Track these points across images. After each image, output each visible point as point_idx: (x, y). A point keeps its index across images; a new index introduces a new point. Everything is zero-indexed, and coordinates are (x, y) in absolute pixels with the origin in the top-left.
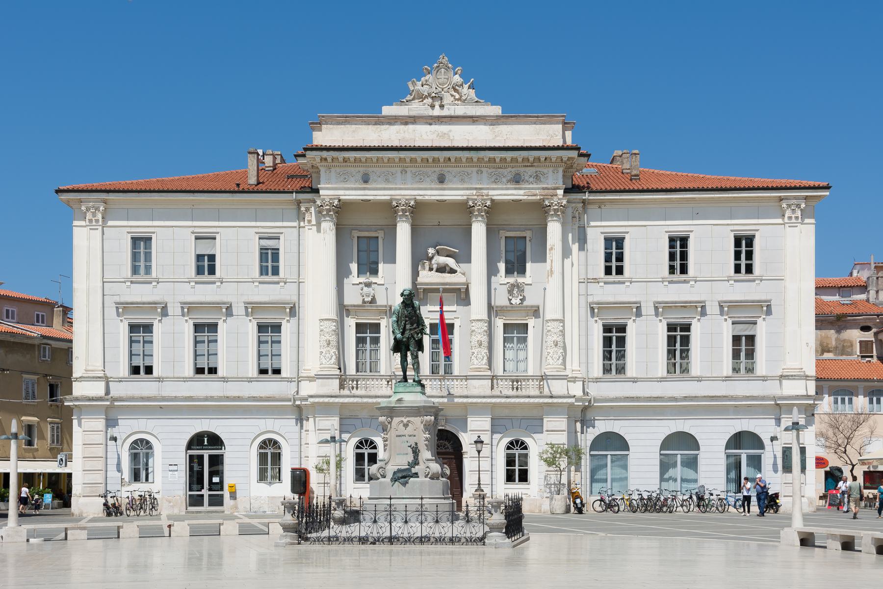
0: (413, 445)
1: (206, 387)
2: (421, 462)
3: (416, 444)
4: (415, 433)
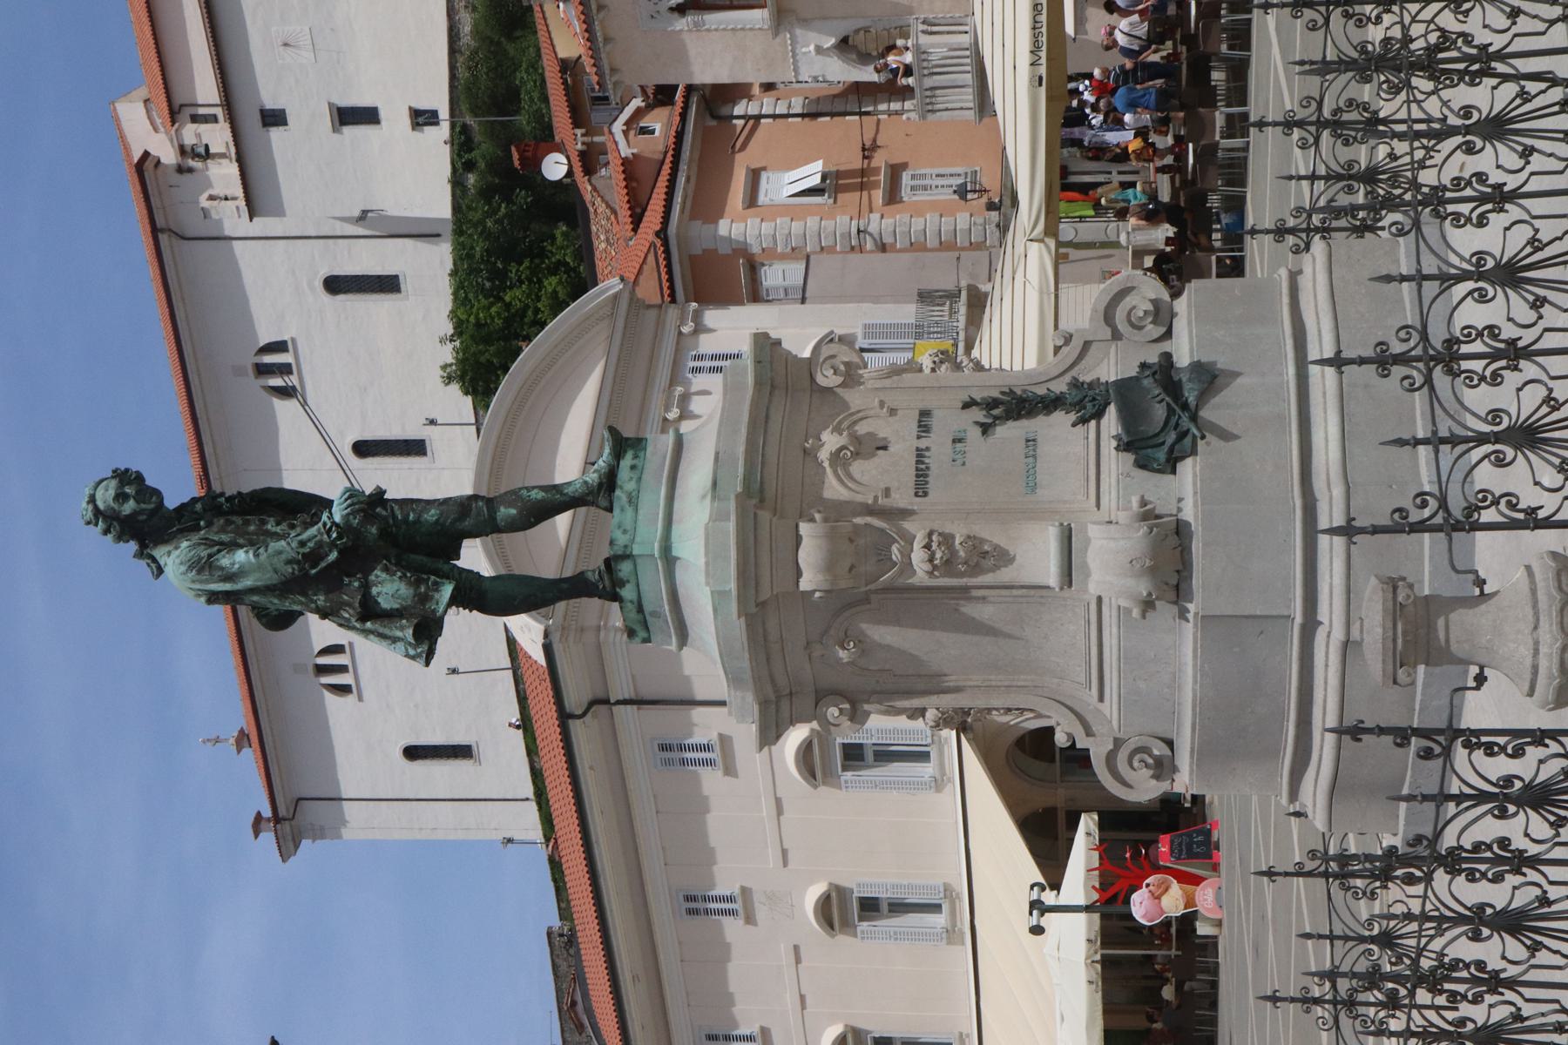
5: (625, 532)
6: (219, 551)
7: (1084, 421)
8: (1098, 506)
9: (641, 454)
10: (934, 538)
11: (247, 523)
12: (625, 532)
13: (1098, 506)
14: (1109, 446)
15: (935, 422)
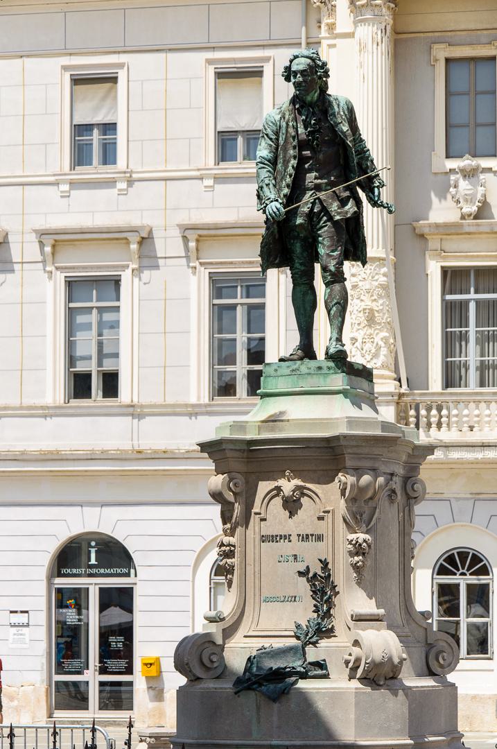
0: (316, 568)
1: (95, 431)
2: (340, 629)
3: (325, 564)
4: (321, 528)
5: (276, 370)
6: (271, 139)
7: (298, 626)
8: (245, 637)
9: (332, 371)
10: (228, 548)
11: (294, 148)
12: (276, 370)
13: (245, 637)
14: (267, 643)
15: (311, 544)
